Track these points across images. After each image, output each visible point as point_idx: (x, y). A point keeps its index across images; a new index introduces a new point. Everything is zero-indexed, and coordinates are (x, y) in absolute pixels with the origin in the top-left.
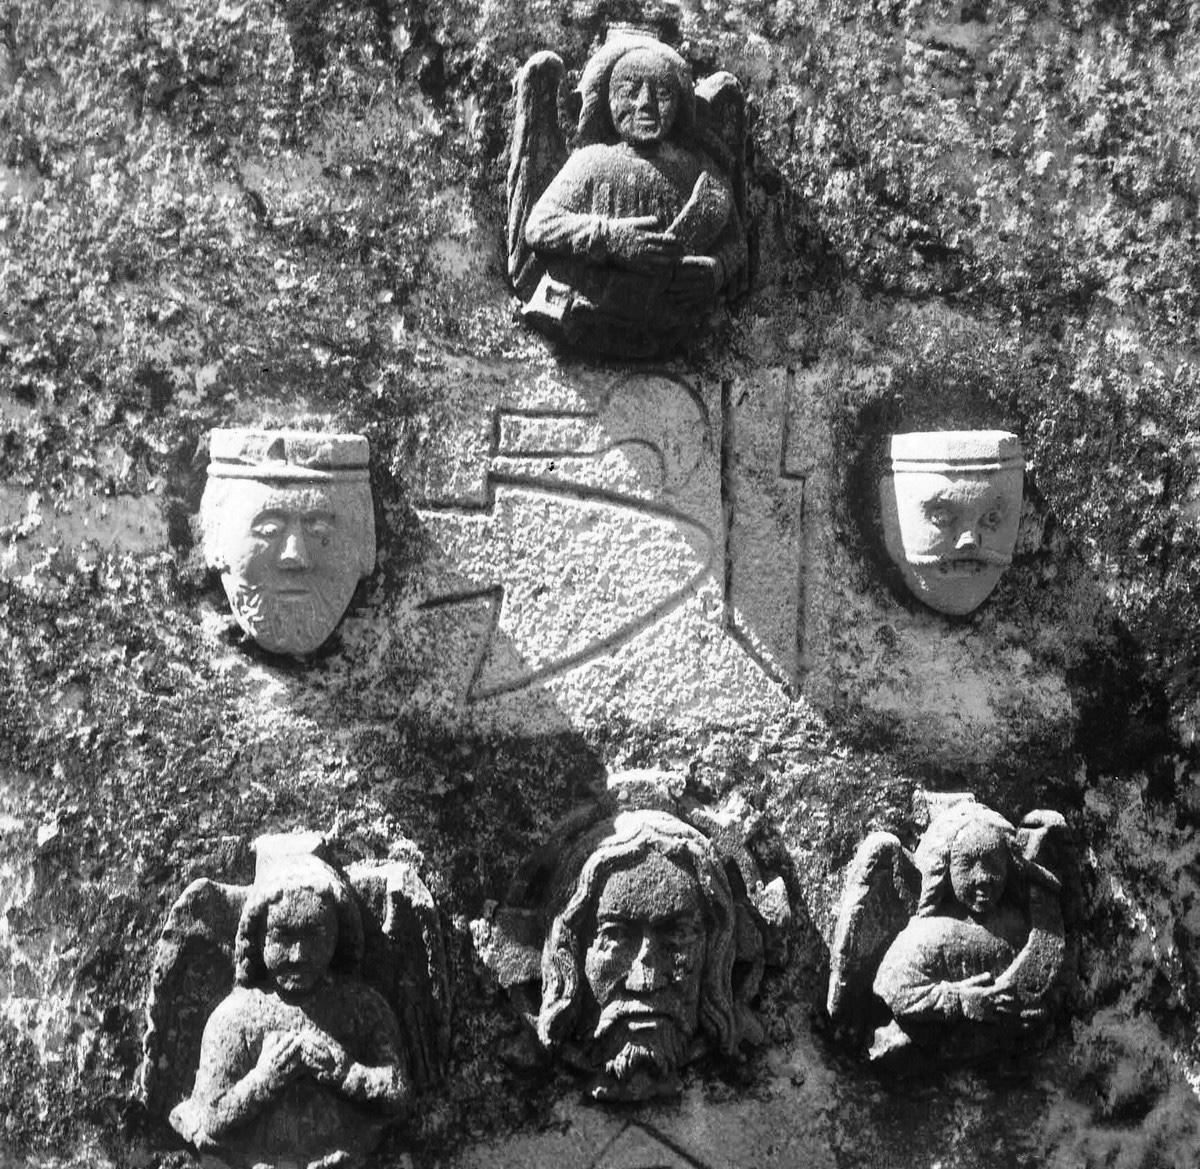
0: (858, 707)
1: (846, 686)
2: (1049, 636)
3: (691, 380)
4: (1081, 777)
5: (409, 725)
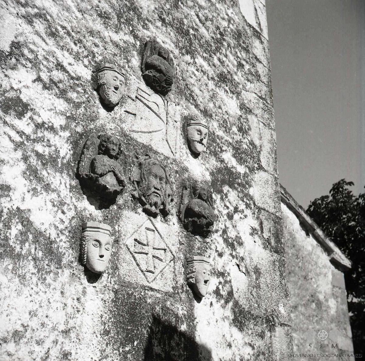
0: (183, 163)
1: (181, 158)
2: (207, 166)
3: (163, 98)
4: (212, 190)
5: (121, 128)
